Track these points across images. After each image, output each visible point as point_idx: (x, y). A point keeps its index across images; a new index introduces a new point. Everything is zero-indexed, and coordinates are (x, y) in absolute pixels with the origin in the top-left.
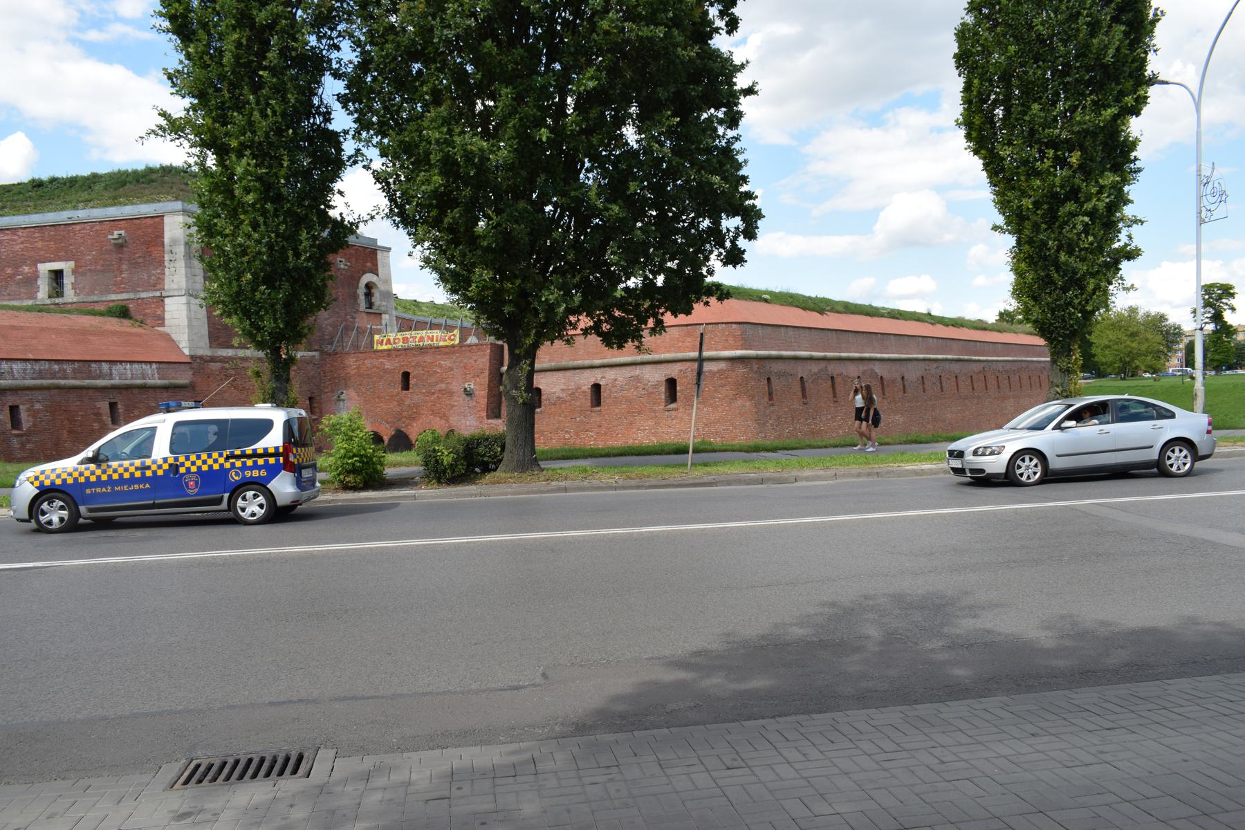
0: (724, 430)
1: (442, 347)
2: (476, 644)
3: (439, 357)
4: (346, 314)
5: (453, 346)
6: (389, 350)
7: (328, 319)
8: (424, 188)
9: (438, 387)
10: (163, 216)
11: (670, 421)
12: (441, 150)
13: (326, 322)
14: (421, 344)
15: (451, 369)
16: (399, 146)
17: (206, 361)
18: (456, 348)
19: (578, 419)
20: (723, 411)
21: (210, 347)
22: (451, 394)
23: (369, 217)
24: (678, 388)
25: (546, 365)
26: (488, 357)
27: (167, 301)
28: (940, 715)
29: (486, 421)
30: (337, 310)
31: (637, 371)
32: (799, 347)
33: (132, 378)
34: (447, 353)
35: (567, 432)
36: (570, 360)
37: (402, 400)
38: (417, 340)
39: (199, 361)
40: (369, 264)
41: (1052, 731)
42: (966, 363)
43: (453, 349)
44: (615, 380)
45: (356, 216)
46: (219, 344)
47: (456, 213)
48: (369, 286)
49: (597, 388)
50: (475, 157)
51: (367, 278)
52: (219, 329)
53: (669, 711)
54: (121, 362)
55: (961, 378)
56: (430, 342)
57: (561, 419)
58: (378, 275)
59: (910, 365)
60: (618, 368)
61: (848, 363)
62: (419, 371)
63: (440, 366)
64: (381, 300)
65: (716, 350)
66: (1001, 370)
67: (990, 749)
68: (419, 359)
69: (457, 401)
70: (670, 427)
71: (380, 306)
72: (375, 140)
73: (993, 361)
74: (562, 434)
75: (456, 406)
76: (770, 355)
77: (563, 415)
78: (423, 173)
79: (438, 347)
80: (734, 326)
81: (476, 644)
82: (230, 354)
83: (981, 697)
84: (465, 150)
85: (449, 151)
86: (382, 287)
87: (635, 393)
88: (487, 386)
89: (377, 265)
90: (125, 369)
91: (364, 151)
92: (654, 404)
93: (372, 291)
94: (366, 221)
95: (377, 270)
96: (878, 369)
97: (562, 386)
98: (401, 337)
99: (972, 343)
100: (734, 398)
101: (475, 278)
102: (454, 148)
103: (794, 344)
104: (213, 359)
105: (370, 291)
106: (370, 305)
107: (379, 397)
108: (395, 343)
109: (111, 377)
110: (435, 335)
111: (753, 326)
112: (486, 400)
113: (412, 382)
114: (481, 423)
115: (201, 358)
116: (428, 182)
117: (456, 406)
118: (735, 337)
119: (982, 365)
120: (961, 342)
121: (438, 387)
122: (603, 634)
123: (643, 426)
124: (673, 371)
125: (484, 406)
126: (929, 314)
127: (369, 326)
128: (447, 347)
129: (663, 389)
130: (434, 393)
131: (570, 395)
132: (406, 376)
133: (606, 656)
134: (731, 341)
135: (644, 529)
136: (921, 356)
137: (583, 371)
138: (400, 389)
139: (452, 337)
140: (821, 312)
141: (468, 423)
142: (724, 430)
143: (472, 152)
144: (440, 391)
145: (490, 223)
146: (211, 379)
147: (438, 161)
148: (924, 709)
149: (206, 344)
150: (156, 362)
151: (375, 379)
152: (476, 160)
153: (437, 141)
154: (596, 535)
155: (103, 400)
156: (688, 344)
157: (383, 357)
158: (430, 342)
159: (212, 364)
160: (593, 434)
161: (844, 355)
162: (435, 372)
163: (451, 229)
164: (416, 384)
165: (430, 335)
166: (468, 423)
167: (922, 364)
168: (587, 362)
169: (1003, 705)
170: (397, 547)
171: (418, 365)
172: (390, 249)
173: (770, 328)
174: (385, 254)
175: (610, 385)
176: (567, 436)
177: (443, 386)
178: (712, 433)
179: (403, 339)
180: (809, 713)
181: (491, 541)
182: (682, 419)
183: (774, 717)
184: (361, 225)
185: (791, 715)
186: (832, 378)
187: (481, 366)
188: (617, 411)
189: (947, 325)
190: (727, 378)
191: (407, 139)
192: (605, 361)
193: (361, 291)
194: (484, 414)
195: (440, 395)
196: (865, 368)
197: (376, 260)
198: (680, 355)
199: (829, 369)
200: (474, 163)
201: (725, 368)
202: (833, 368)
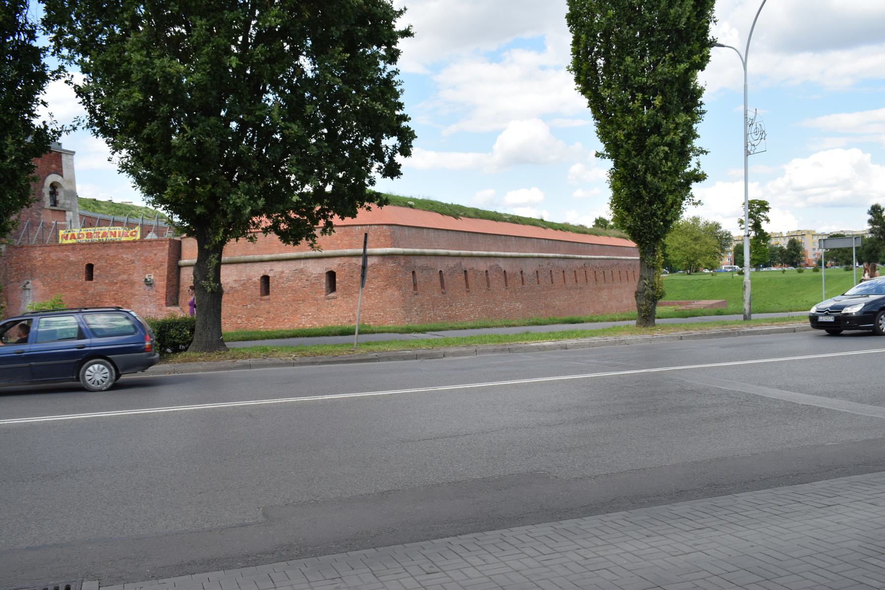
0: (376, 315)
1: (124, 242)
2: (201, 493)
3: (121, 251)
5: (134, 241)
6: (73, 244)
8: (124, 102)
9: (120, 278)
11: (330, 308)
12: (142, 71)
14: (104, 239)
15: (133, 262)
16: (102, 64)
18: (137, 243)
19: (249, 306)
20: (375, 299)
22: (133, 284)
23: (71, 128)
24: (337, 280)
25: (354, 260)
26: (167, 252)
28: (580, 527)
29: (165, 308)
31: (301, 265)
32: (438, 245)
34: (129, 248)
35: (239, 317)
36: (242, 255)
37: (86, 289)
38: (100, 235)
40: (54, 166)
41: (661, 533)
42: (571, 261)
43: (134, 244)
44: (282, 272)
45: (59, 126)
47: (154, 125)
48: (54, 186)
49: (266, 279)
50: (173, 78)
53: (373, 536)
55: (567, 273)
56: (113, 238)
57: (234, 306)
58: (62, 176)
59: (528, 261)
60: (284, 262)
61: (478, 259)
62: (103, 263)
63: (122, 259)
64: (65, 199)
66: (598, 266)
67: (628, 535)
68: (103, 252)
69: (138, 290)
70: (330, 313)
71: (64, 204)
72: (78, 58)
73: (591, 259)
74: (234, 320)
75: (137, 295)
76: (414, 252)
77: (235, 303)
78: (123, 90)
79: (120, 242)
80: (385, 227)
81: (201, 493)
83: (608, 513)
84: (164, 72)
85: (149, 72)
86: (66, 187)
87: (300, 284)
88: (165, 277)
89: (62, 167)
91: (67, 67)
92: (316, 293)
93: (57, 190)
94: (69, 131)
95: (62, 171)
96: (502, 264)
97: (235, 278)
98: (85, 233)
99: (576, 244)
100: (385, 288)
101: (170, 182)
102: (153, 69)
103: (434, 243)
105: (55, 190)
106: (55, 203)
107: (64, 287)
108: (79, 238)
110: (117, 231)
111: (401, 228)
112: (165, 290)
113: (96, 273)
114: (160, 310)
116: (129, 97)
117: (137, 295)
118: (385, 236)
119: (583, 262)
120: (567, 243)
121: (120, 278)
122: (308, 481)
123: (306, 312)
124: (333, 265)
125: (164, 295)
126: (542, 220)
127: (54, 222)
128: (129, 242)
129: (324, 280)
130: (117, 283)
131: (242, 285)
132: (90, 268)
133: (313, 497)
134: (382, 240)
135: (326, 397)
136: (536, 254)
137: (253, 264)
138: (84, 279)
139: (134, 234)
140: (456, 217)
141: (148, 310)
143: (170, 74)
144: (122, 281)
145: (185, 135)
147: (139, 80)
148: (569, 524)
151: (60, 270)
152: (174, 81)
153: (138, 62)
154: (286, 403)
156: (346, 242)
157: (68, 250)
158: (113, 238)
160: (262, 319)
161: (475, 253)
162: (118, 264)
163: (149, 140)
164: (99, 275)
165: (113, 231)
166: (148, 310)
167: (536, 260)
168: (257, 257)
169: (624, 517)
170: (110, 416)
171: (101, 257)
172: (74, 152)
173: (414, 230)
174: (69, 157)
175: (278, 277)
176: (239, 321)
177: (125, 277)
178: (366, 318)
179: (87, 234)
180: (482, 531)
181: (195, 410)
182: (341, 306)
183: (456, 536)
184: (64, 134)
185: (469, 533)
186: (465, 271)
187: (160, 259)
188: (284, 299)
189: (556, 229)
190: (378, 271)
191: (109, 59)
192: (274, 256)
194: (163, 302)
195: (122, 285)
196: (492, 264)
197: (61, 162)
198: (339, 252)
199: (463, 264)
200: (171, 84)
201: (377, 263)
202: (466, 264)
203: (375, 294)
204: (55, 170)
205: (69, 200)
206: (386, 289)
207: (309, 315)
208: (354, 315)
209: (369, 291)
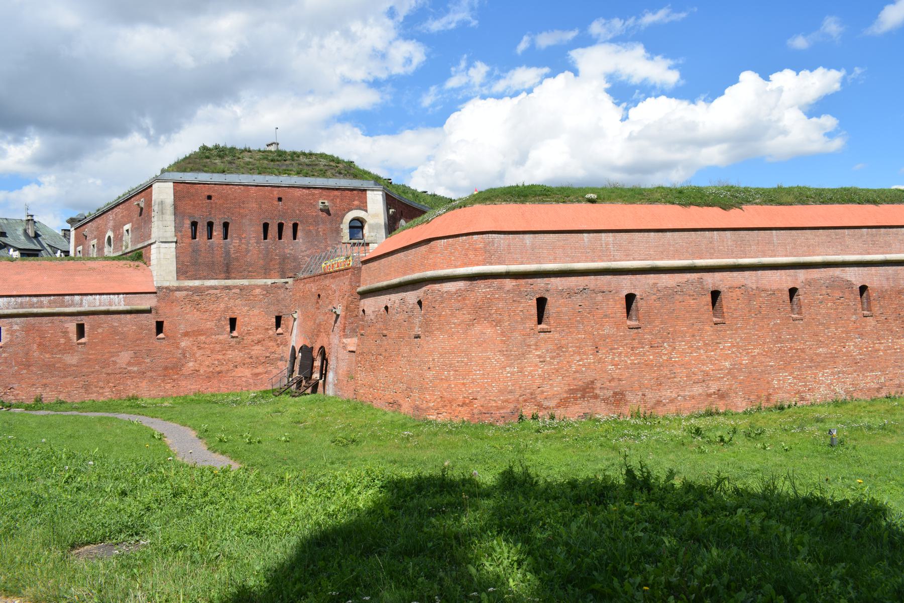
0: (458, 362)
4: (326, 247)
7: (306, 251)
10: (151, 186)
13: (302, 254)
21: (177, 279)
30: (316, 243)
33: (100, 305)
39: (165, 290)
40: (356, 203)
46: (187, 277)
52: (187, 266)
54: (91, 294)
58: (366, 211)
64: (370, 232)
82: (196, 285)
89: (366, 203)
90: (95, 299)
100: (470, 324)
104: (178, 289)
109: (81, 305)
115: (167, 288)
118: (476, 250)
140: (725, 207)
142: (458, 362)
146: (175, 304)
149: (173, 277)
150: (123, 294)
155: (71, 321)
159: (177, 292)
178: (446, 366)
190: (464, 299)
203: (458, 332)
205: (373, 232)
206: (473, 325)
208: (434, 360)
209: (451, 328)
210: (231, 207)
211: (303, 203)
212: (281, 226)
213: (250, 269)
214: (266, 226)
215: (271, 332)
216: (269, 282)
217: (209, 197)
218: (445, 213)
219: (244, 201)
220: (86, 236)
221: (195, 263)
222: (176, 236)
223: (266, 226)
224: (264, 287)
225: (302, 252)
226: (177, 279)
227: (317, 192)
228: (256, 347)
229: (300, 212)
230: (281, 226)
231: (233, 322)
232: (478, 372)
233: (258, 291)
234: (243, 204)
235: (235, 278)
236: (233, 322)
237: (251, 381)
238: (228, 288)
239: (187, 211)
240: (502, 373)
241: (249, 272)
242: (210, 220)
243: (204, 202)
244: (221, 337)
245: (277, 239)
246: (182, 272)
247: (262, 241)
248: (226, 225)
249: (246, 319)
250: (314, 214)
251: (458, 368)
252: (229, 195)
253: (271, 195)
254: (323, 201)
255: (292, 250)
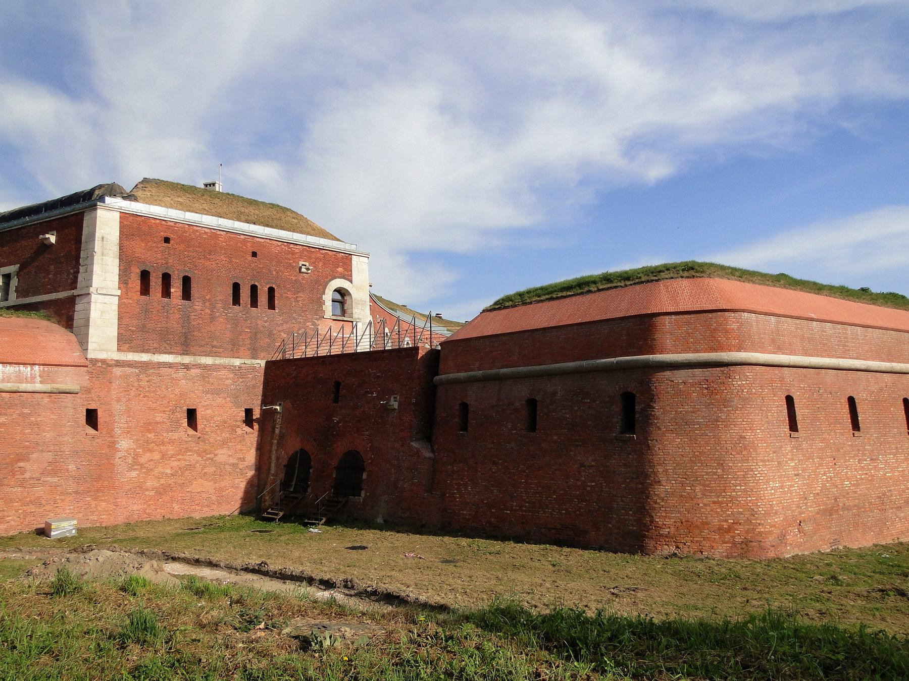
7: (282, 324)
10: (84, 212)
13: (277, 328)
17: (109, 366)
27: (78, 300)
40: (340, 270)
48: (339, 291)
49: (532, 404)
51: (338, 283)
52: (132, 331)
58: (351, 282)
65: (698, 351)
104: (119, 364)
113: (343, 392)
115: (103, 361)
132: (338, 384)
193: (328, 296)
204: (341, 274)
207: (592, 466)
210: (194, 257)
211: (281, 263)
212: (254, 289)
213: (215, 343)
214: (236, 287)
215: (238, 430)
216: (237, 362)
217: (167, 240)
218: (631, 285)
219: (210, 251)
220: (87, 272)
221: (143, 329)
222: (119, 288)
223: (236, 287)
224: (231, 368)
225: (278, 326)
226: (119, 350)
227: (297, 251)
228: (220, 451)
229: (277, 273)
230: (254, 289)
231: (191, 415)
232: (739, 488)
233: (223, 373)
234: (210, 254)
235: (195, 355)
236: (191, 415)
237: (214, 498)
238: (187, 367)
239: (137, 255)
240: (766, 488)
241: (213, 347)
242: (167, 271)
243: (160, 245)
244: (175, 436)
245: (249, 306)
246: (125, 340)
247: (231, 306)
248: (187, 281)
249: (209, 412)
250: (294, 278)
251: (707, 482)
252: (192, 239)
253: (244, 247)
254: (304, 263)
255: (266, 322)
